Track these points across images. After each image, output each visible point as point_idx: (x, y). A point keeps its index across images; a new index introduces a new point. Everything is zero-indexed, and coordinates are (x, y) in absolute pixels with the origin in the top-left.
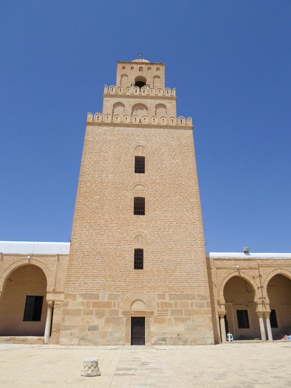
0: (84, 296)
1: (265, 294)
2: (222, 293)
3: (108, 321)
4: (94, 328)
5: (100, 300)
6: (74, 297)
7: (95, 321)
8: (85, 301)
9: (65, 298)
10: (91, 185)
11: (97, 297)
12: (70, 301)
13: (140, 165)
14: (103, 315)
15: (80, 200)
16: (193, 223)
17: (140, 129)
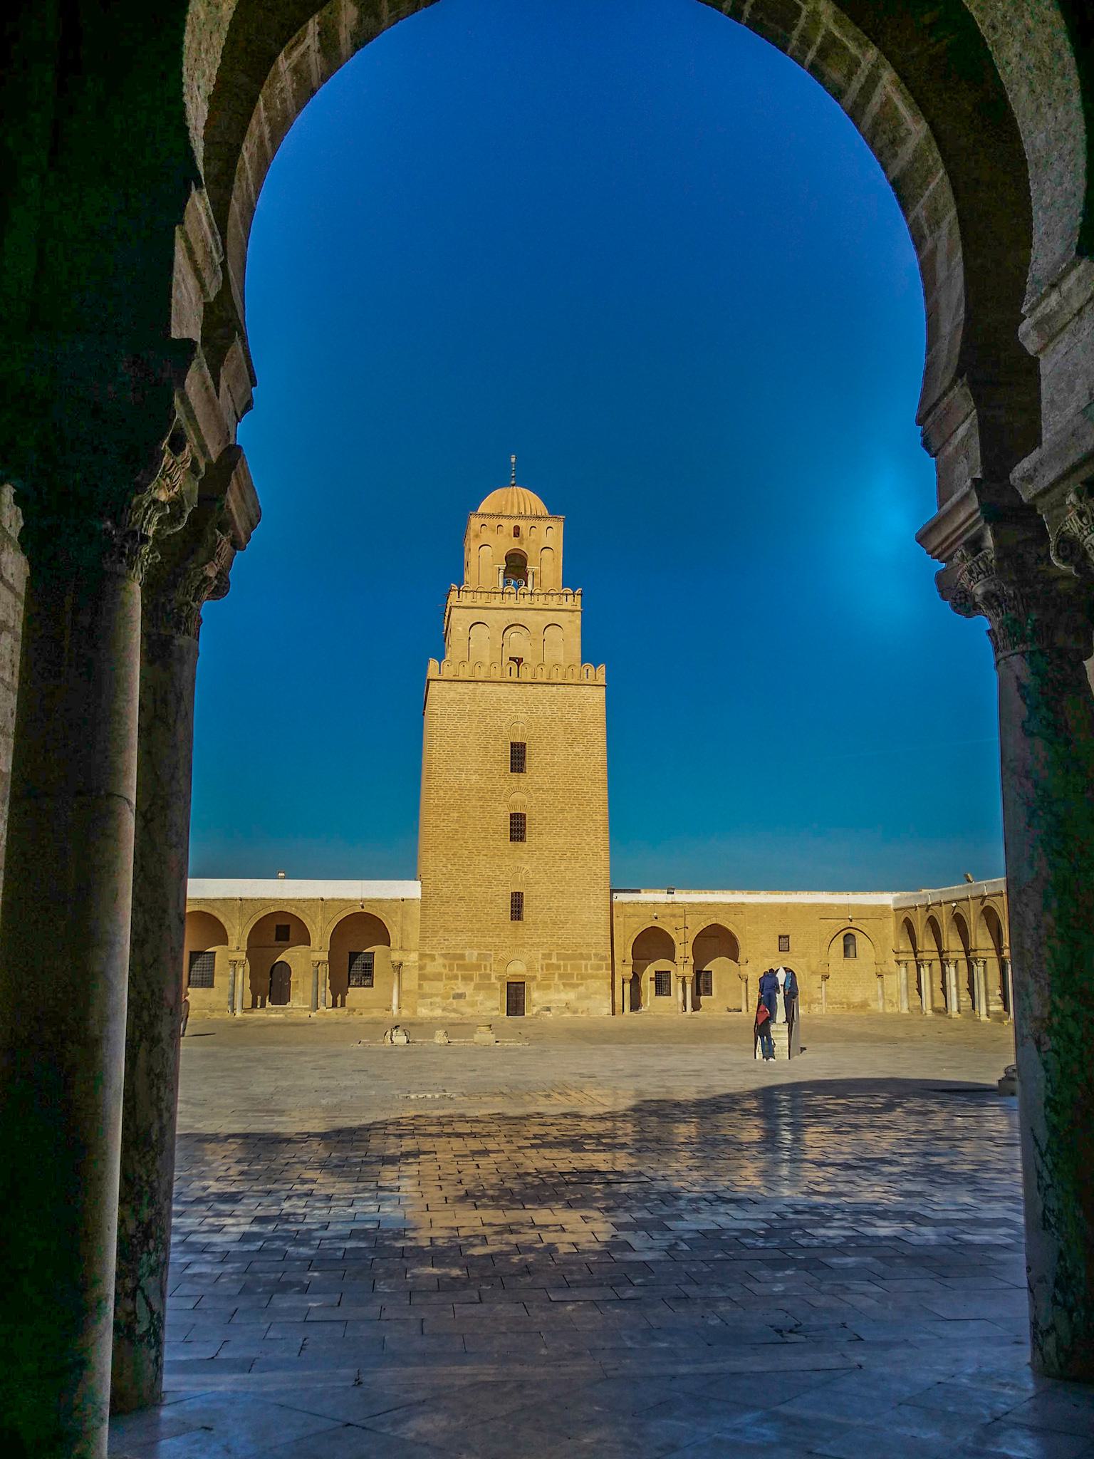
0: (445, 956)
1: (689, 953)
2: (630, 951)
3: (478, 988)
4: (460, 996)
5: (467, 961)
6: (433, 957)
7: (460, 987)
8: (447, 962)
9: (420, 959)
10: (445, 793)
11: (462, 957)
12: (427, 961)
13: (518, 757)
14: (472, 980)
15: (428, 816)
16: (595, 854)
17: (518, 689)
